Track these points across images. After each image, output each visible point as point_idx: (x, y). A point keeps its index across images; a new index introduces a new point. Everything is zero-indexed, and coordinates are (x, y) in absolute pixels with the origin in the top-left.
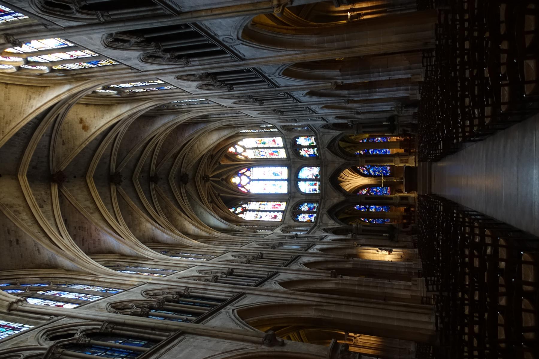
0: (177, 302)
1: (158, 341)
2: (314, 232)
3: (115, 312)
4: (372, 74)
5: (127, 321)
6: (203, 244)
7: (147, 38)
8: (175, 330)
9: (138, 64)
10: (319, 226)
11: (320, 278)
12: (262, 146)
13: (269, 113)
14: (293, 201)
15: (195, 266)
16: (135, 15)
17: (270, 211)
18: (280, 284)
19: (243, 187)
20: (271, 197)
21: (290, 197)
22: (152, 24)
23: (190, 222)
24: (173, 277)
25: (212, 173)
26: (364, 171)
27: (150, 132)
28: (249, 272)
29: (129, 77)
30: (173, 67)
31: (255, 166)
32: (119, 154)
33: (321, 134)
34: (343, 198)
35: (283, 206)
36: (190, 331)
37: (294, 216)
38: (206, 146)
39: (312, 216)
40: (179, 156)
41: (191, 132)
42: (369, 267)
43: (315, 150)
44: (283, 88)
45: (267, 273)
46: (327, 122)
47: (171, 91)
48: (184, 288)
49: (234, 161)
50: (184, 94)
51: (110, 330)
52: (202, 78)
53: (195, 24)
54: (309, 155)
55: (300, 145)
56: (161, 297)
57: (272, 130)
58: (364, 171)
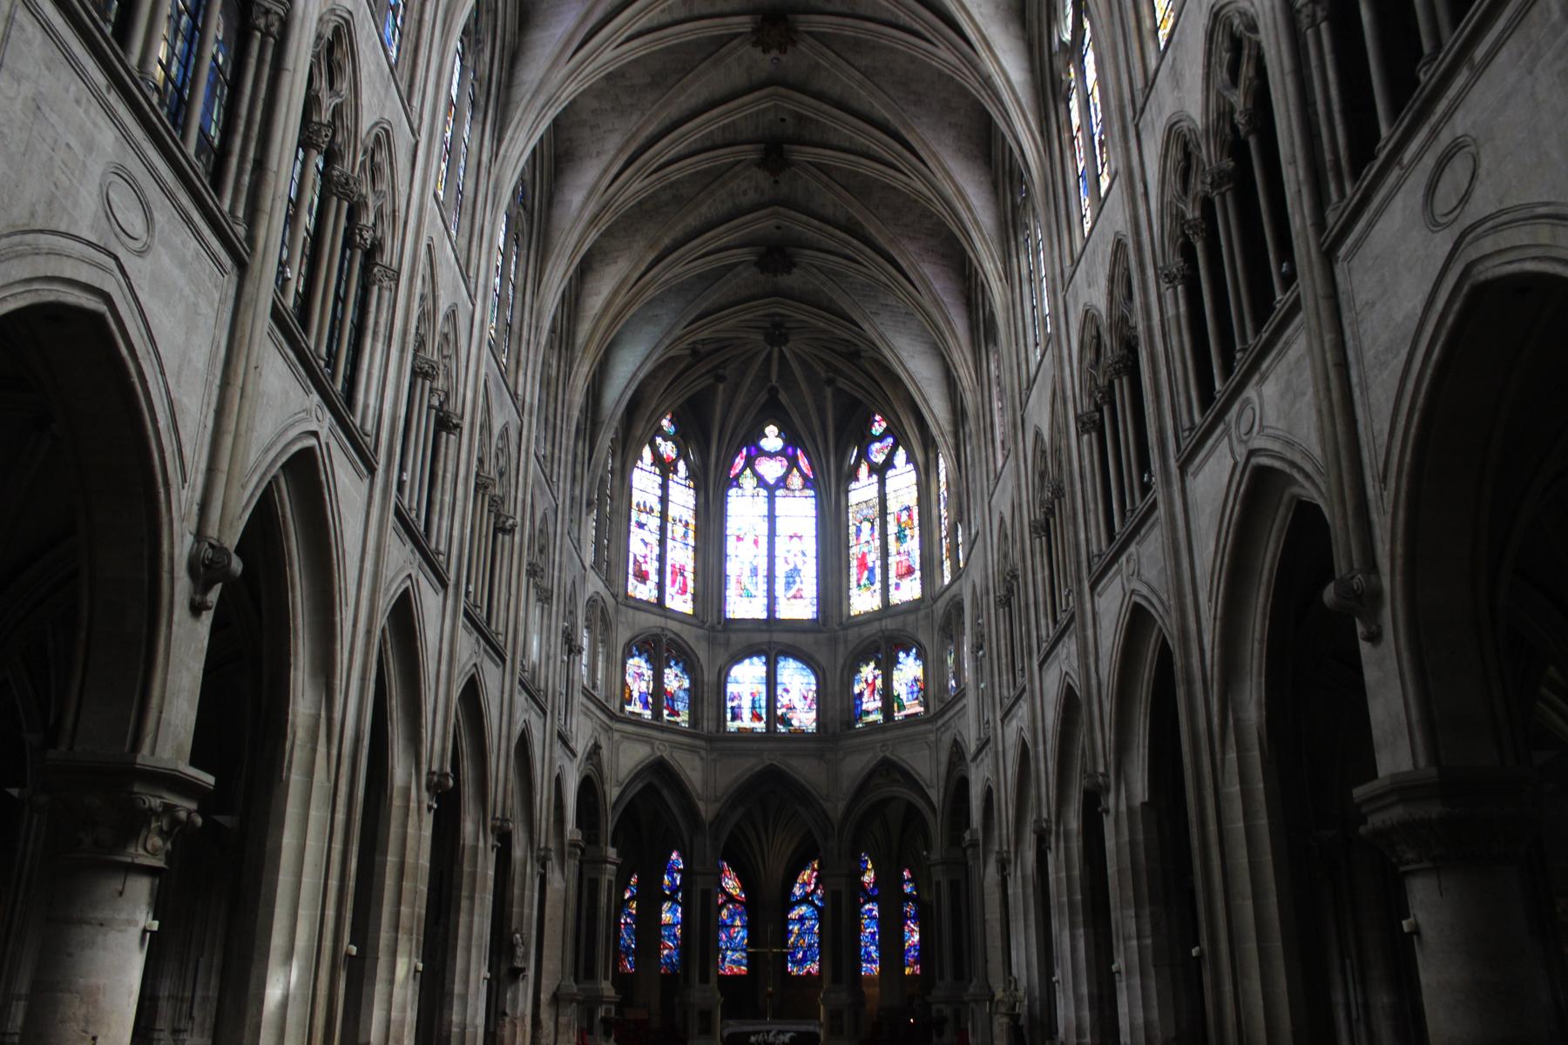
0: (348, 242)
1: (217, 183)
2: (587, 713)
3: (319, 37)
4: (1132, 912)
5: (286, 79)
6: (546, 324)
7: (1247, 144)
8: (251, 238)
9: (1160, 113)
10: (608, 729)
11: (426, 734)
12: (892, 528)
13: (1006, 556)
14: (698, 639)
15: (473, 298)
16: (1320, 108)
17: (662, 558)
18: (406, 592)
19: (750, 463)
20: (712, 560)
21: (712, 628)
22: (1294, 162)
23: (623, 282)
24: (433, 223)
25: (797, 356)
26: (804, 884)
27: (935, 147)
28: (448, 486)
29: (1119, 79)
30: (1156, 228)
31: (820, 507)
32: (857, 45)
33: (932, 737)
34: (707, 811)
35: (681, 603)
36: (249, 288)
37: (646, 642)
38: (889, 335)
39: (646, 705)
40: (855, 242)
41: (938, 286)
42: (464, 904)
43: (877, 717)
44: (1088, 606)
45: (442, 548)
46: (974, 758)
47: (1076, 219)
48: (395, 265)
49: (839, 431)
50: (1068, 262)
51: (262, 22)
52: (1122, 325)
53: (1295, 308)
54: (861, 694)
55: (896, 661)
56: (366, 189)
57: (947, 564)
58: (804, 884)
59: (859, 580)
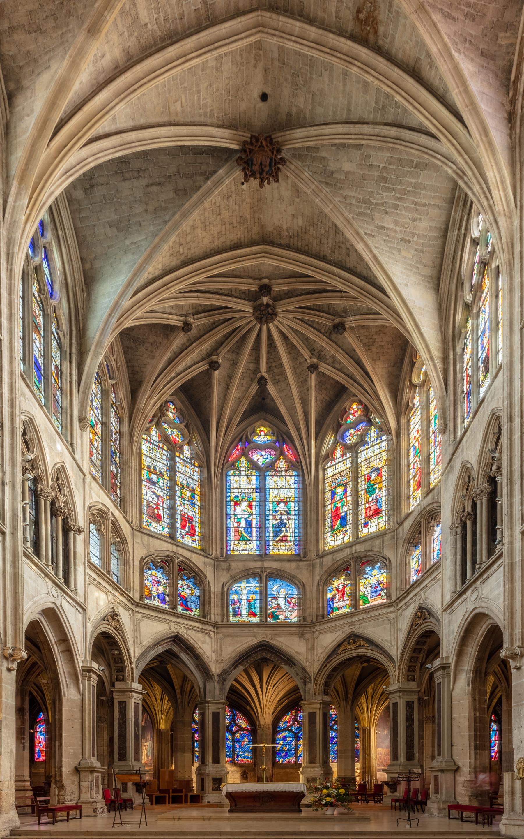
20: (215, 514)
59: (333, 526)
